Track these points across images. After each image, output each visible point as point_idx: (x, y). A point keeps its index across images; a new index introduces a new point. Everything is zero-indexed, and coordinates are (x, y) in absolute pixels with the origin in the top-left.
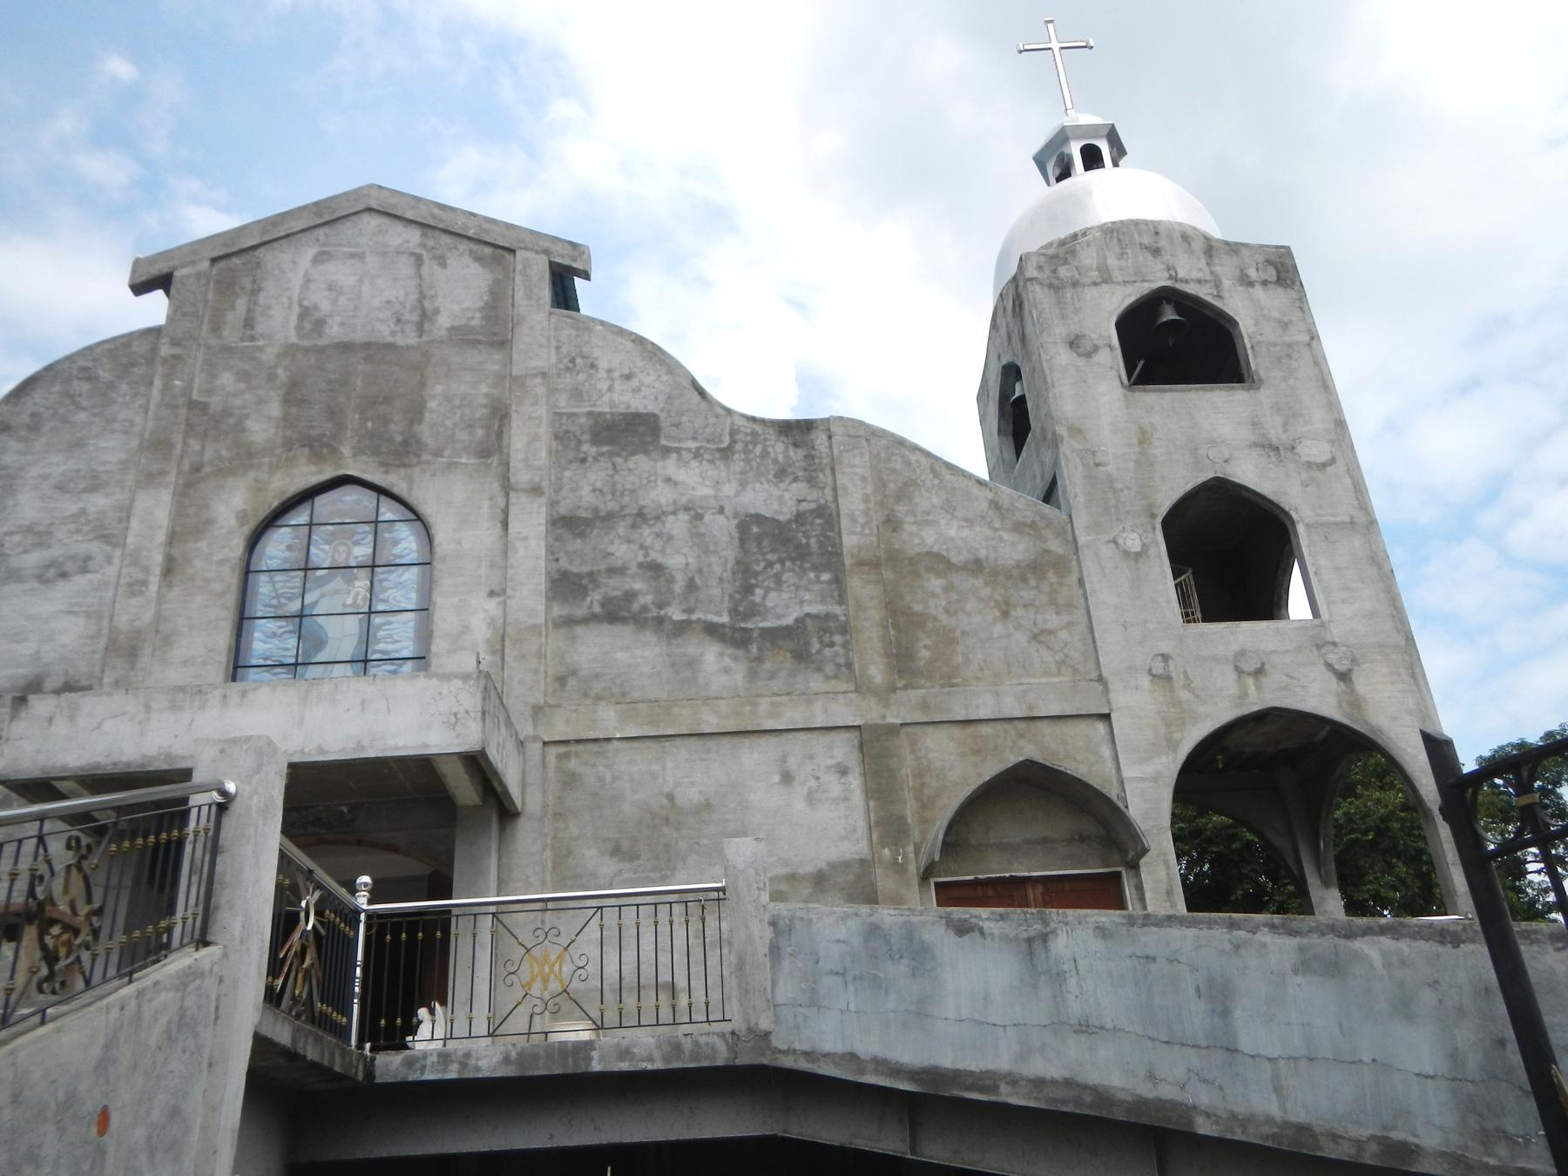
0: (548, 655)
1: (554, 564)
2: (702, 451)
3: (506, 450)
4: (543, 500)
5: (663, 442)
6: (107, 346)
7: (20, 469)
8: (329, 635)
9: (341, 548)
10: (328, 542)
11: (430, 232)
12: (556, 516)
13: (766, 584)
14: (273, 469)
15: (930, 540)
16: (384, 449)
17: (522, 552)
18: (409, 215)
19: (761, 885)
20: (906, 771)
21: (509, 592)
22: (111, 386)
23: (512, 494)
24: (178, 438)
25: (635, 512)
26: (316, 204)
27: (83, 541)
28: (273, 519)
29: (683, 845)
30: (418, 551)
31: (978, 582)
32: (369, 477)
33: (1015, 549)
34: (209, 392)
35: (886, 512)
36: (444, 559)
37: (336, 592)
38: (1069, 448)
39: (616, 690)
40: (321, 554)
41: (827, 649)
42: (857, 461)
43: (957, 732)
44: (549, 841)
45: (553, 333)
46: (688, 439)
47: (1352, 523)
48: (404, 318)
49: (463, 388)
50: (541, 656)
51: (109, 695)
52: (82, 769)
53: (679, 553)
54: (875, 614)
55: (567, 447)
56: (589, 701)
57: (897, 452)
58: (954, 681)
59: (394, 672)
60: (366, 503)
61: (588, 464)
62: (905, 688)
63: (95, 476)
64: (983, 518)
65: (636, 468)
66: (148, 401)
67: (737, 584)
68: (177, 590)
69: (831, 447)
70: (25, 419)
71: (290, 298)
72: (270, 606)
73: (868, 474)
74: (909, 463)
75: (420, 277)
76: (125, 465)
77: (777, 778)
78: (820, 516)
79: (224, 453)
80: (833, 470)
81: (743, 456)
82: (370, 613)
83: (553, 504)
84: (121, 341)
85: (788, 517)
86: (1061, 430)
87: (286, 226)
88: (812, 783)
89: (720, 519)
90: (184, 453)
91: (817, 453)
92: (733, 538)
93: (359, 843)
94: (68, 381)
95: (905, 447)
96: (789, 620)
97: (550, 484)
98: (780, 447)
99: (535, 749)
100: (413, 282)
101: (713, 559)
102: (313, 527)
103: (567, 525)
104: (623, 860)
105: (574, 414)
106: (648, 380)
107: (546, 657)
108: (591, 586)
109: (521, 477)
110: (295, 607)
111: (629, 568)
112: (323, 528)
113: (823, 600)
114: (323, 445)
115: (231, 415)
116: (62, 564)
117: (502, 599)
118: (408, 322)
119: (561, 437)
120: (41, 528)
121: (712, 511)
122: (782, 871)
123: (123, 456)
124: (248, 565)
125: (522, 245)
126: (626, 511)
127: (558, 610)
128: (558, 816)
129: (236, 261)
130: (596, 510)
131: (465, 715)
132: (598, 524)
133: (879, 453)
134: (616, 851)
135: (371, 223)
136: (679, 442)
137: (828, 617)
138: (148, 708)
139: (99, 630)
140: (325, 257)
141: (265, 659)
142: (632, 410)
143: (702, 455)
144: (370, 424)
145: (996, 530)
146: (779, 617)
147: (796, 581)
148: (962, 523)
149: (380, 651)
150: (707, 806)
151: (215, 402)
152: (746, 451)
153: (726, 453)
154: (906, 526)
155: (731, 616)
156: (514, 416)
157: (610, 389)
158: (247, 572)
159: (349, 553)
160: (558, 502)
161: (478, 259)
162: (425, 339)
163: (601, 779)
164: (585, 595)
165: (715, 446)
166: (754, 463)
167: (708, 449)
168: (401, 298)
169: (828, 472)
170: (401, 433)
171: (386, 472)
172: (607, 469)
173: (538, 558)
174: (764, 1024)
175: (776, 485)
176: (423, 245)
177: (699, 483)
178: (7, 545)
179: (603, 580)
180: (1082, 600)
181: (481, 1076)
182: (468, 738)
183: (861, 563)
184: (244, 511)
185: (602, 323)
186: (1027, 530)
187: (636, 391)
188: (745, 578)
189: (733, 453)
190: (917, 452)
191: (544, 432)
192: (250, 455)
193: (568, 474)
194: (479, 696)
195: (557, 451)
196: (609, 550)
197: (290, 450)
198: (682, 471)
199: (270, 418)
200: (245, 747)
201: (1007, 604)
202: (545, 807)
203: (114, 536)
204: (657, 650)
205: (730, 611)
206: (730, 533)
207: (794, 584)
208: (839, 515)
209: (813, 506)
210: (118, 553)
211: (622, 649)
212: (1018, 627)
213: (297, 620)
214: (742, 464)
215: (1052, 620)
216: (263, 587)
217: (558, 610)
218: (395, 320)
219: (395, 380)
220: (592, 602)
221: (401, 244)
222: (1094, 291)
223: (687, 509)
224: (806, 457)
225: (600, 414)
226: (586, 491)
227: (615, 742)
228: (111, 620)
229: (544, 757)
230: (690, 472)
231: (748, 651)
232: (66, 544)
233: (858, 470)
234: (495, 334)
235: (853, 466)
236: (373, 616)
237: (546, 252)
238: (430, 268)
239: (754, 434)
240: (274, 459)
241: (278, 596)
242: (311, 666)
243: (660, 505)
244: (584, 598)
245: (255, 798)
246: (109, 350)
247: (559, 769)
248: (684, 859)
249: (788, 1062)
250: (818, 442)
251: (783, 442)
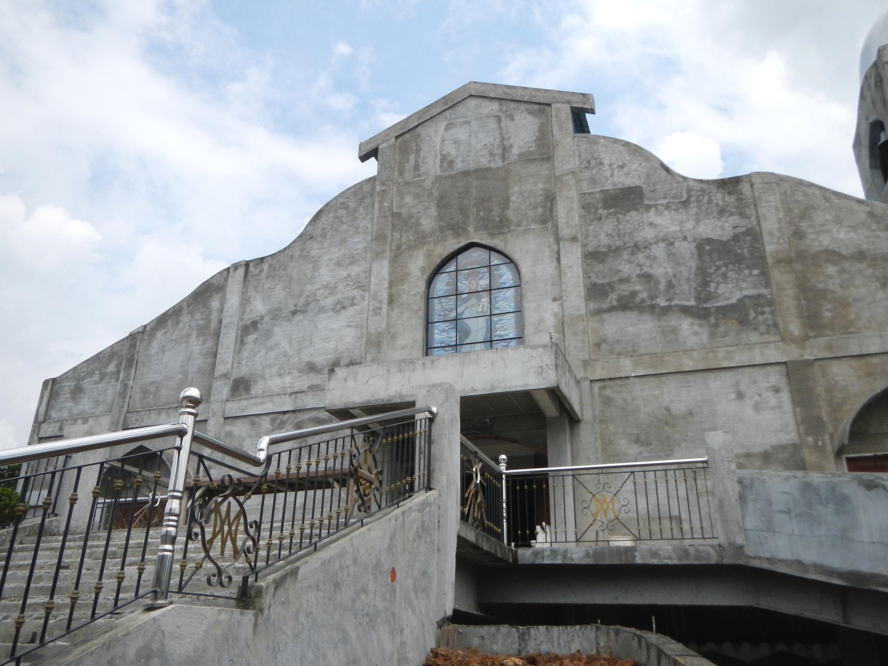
0: (589, 332)
1: (588, 280)
2: (670, 205)
3: (555, 218)
4: (579, 244)
5: (646, 202)
6: (352, 190)
7: (320, 257)
8: (472, 328)
9: (473, 282)
10: (466, 279)
11: (503, 102)
12: (587, 252)
13: (717, 280)
14: (436, 243)
16: (490, 226)
17: (569, 275)
18: (492, 95)
19: (730, 459)
20: (820, 388)
21: (564, 298)
22: (355, 210)
23: (561, 243)
24: (389, 233)
25: (632, 245)
26: (443, 98)
27: (350, 290)
28: (438, 270)
29: (677, 436)
30: (513, 280)
31: (863, 266)
32: (483, 242)
34: (401, 207)
35: (794, 228)
36: (527, 282)
37: (473, 305)
39: (629, 349)
40: (463, 286)
43: (854, 362)
44: (598, 435)
45: (576, 148)
46: (661, 199)
48: (494, 153)
49: (529, 187)
50: (585, 332)
51: (371, 366)
52: (361, 403)
53: (661, 266)
54: (791, 292)
55: (590, 213)
56: (615, 356)
57: (798, 189)
58: (850, 330)
59: (507, 346)
60: (484, 256)
61: (602, 221)
62: (815, 337)
63: (353, 257)
64: (863, 224)
65: (631, 220)
66: (373, 216)
67: (699, 281)
68: (396, 311)
69: (753, 192)
70: (319, 232)
71: (435, 151)
72: (441, 316)
74: (807, 195)
75: (501, 129)
76: (365, 248)
77: (733, 396)
78: (749, 235)
79: (411, 238)
80: (756, 206)
81: (696, 204)
82: (491, 315)
83: (584, 246)
84: (358, 186)
85: (728, 238)
87: (430, 113)
88: (757, 398)
89: (685, 244)
90: (392, 240)
91: (744, 197)
92: (693, 254)
93: (496, 438)
94: (336, 211)
95: (804, 185)
96: (734, 301)
97: (582, 234)
98: (719, 196)
99: (586, 385)
100: (498, 132)
101: (682, 268)
102: (458, 272)
103: (593, 257)
104: (642, 445)
105: (593, 193)
106: (634, 167)
107: (588, 333)
108: (610, 290)
109: (565, 232)
110: (453, 315)
111: (632, 278)
112: (463, 272)
113: (755, 287)
114: (458, 228)
115: (413, 217)
116: (342, 302)
117: (561, 302)
118: (496, 154)
119: (585, 207)
120: (331, 286)
121: (681, 239)
122: (741, 451)
123: (364, 245)
124: (428, 295)
125: (555, 101)
126: (627, 245)
127: (592, 306)
128: (602, 421)
129: (407, 136)
130: (609, 247)
131: (547, 367)
132: (611, 254)
133: (786, 191)
134: (637, 441)
135: (472, 102)
136: (656, 201)
137: (759, 296)
138: (388, 371)
139: (363, 334)
140: (451, 126)
141: (441, 343)
142: (626, 186)
143: (670, 207)
144: (482, 213)
145: (873, 231)
146: (727, 299)
147: (736, 276)
148: (847, 229)
149: (497, 336)
150: (691, 414)
151: (404, 212)
152: (698, 201)
153: (685, 204)
154: (808, 235)
155: (696, 301)
156: (558, 198)
157: (612, 175)
158: (428, 299)
159: (477, 284)
160: (587, 244)
161: (531, 113)
162: (506, 162)
163: (625, 400)
164: (608, 296)
165: (679, 201)
166: (703, 208)
167: (674, 203)
168: (492, 142)
169: (752, 207)
170: (498, 216)
171: (493, 238)
172: (614, 222)
173: (579, 277)
174: (740, 540)
175: (718, 219)
176: (501, 111)
177: (670, 224)
178: (318, 295)
179: (617, 286)
181: (574, 563)
182: (549, 379)
183: (779, 261)
184: (424, 267)
185: (604, 138)
187: (627, 174)
188: (703, 278)
189: (690, 203)
190: (813, 187)
191: (576, 205)
192: (424, 237)
193: (591, 228)
194: (553, 356)
195: (584, 215)
196: (619, 269)
197: (443, 232)
198: (659, 218)
199: (431, 216)
200: (439, 389)
202: (594, 417)
203: (364, 286)
204: (652, 324)
206: (691, 251)
207: (735, 278)
208: (761, 233)
209: (744, 229)
210: (367, 294)
211: (633, 325)
213: (455, 322)
214: (696, 209)
216: (437, 306)
217: (592, 306)
218: (489, 155)
219: (493, 188)
220: (611, 299)
221: (489, 112)
223: (664, 240)
224: (737, 200)
225: (607, 191)
226: (603, 236)
227: (632, 379)
228: (367, 329)
229: (591, 389)
230: (664, 218)
231: (709, 321)
232: (343, 292)
233: (770, 204)
234: (544, 154)
235: (769, 202)
236: (493, 317)
237: (569, 102)
238: (505, 122)
239: (702, 190)
240: (436, 238)
241: (444, 310)
242: (464, 346)
243: (647, 239)
244: (607, 298)
245: (446, 415)
246: (353, 192)
247: (600, 395)
248: (679, 445)
249: (756, 564)
250: (743, 190)
251: (721, 193)
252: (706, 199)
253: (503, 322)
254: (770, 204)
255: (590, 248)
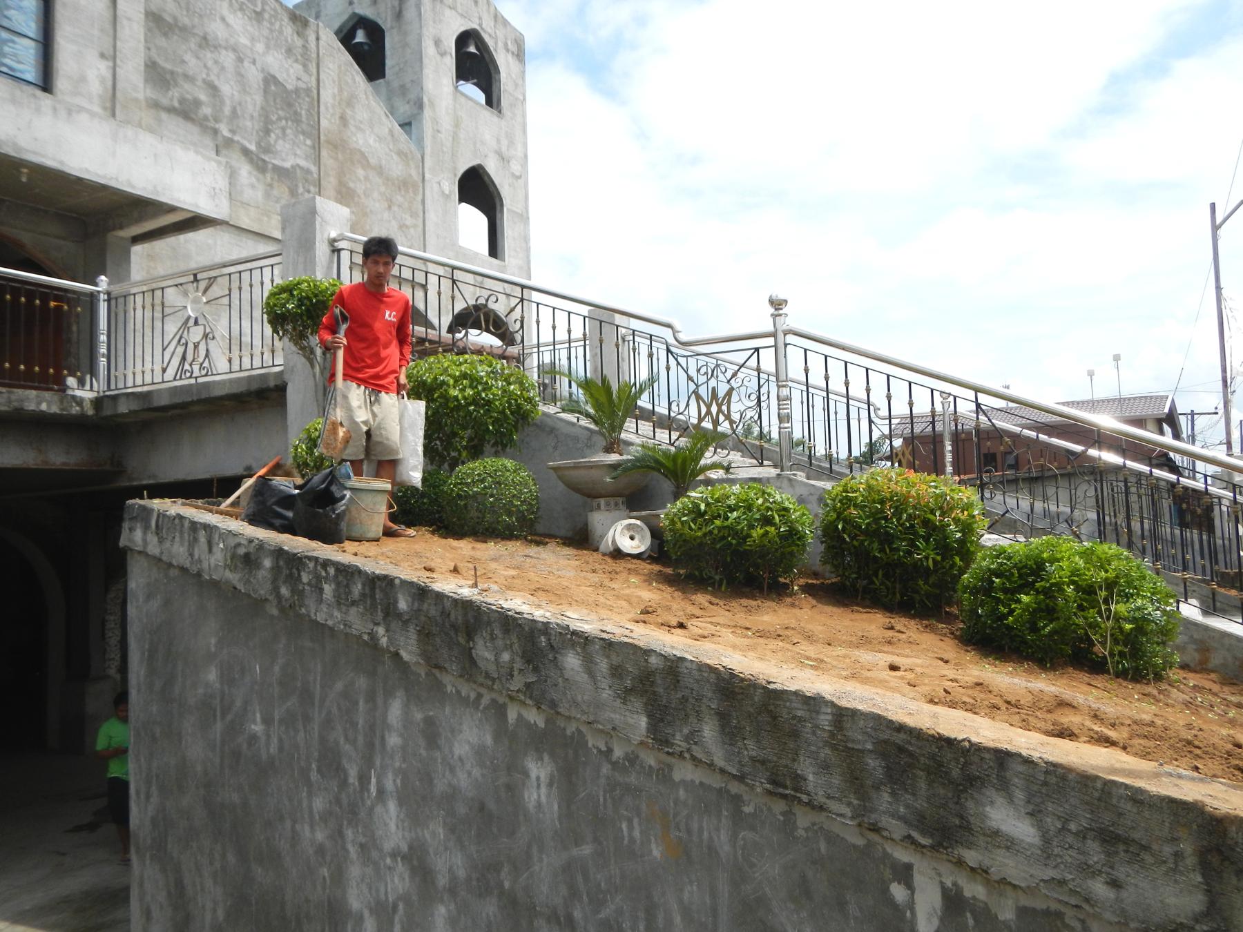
13: (277, 131)
15: (361, 142)
33: (396, 168)
38: (427, 112)
41: (306, 194)
42: (331, 66)
47: (522, 215)
73: (336, 79)
78: (308, 96)
81: (268, 25)
86: (425, 99)
89: (252, 67)
96: (287, 165)
101: (249, 99)
108: (172, 82)
113: (307, 158)
126: (196, 31)
130: (175, 19)
137: (308, 171)
146: (283, 160)
153: (258, 16)
164: (169, 89)
179: (181, 81)
180: (422, 213)
183: (328, 142)
186: (403, 157)
196: (184, 58)
198: (232, 16)
201: (391, 202)
205: (256, 143)
209: (304, 86)
212: (395, 218)
214: (267, 31)
215: (409, 221)
222: (448, 12)
223: (234, 50)
233: (331, 73)
235: (329, 68)
252: (277, 26)
253: (17, 46)
254: (331, 73)
255: (153, 8)
